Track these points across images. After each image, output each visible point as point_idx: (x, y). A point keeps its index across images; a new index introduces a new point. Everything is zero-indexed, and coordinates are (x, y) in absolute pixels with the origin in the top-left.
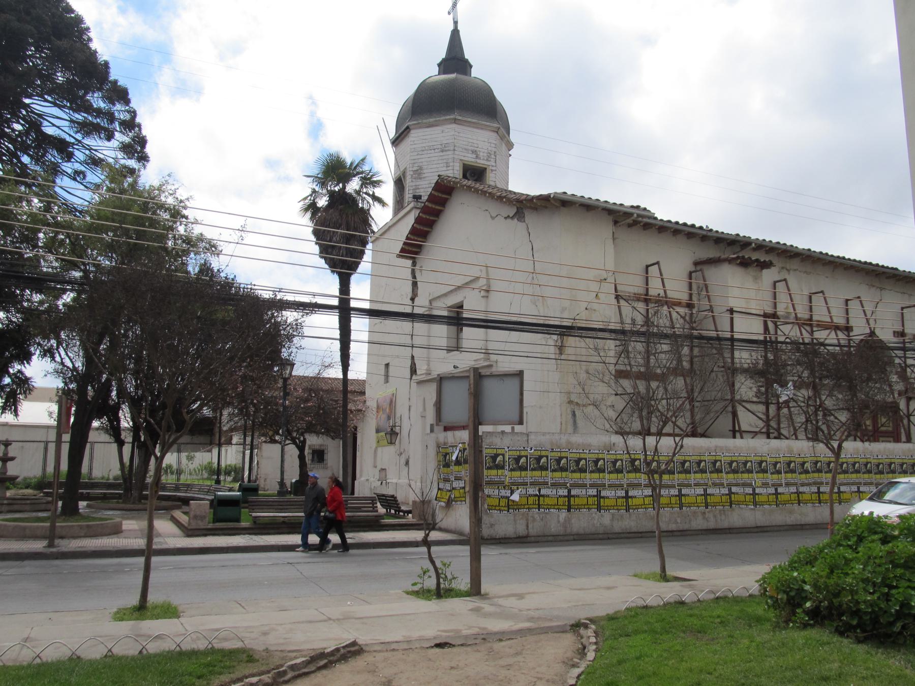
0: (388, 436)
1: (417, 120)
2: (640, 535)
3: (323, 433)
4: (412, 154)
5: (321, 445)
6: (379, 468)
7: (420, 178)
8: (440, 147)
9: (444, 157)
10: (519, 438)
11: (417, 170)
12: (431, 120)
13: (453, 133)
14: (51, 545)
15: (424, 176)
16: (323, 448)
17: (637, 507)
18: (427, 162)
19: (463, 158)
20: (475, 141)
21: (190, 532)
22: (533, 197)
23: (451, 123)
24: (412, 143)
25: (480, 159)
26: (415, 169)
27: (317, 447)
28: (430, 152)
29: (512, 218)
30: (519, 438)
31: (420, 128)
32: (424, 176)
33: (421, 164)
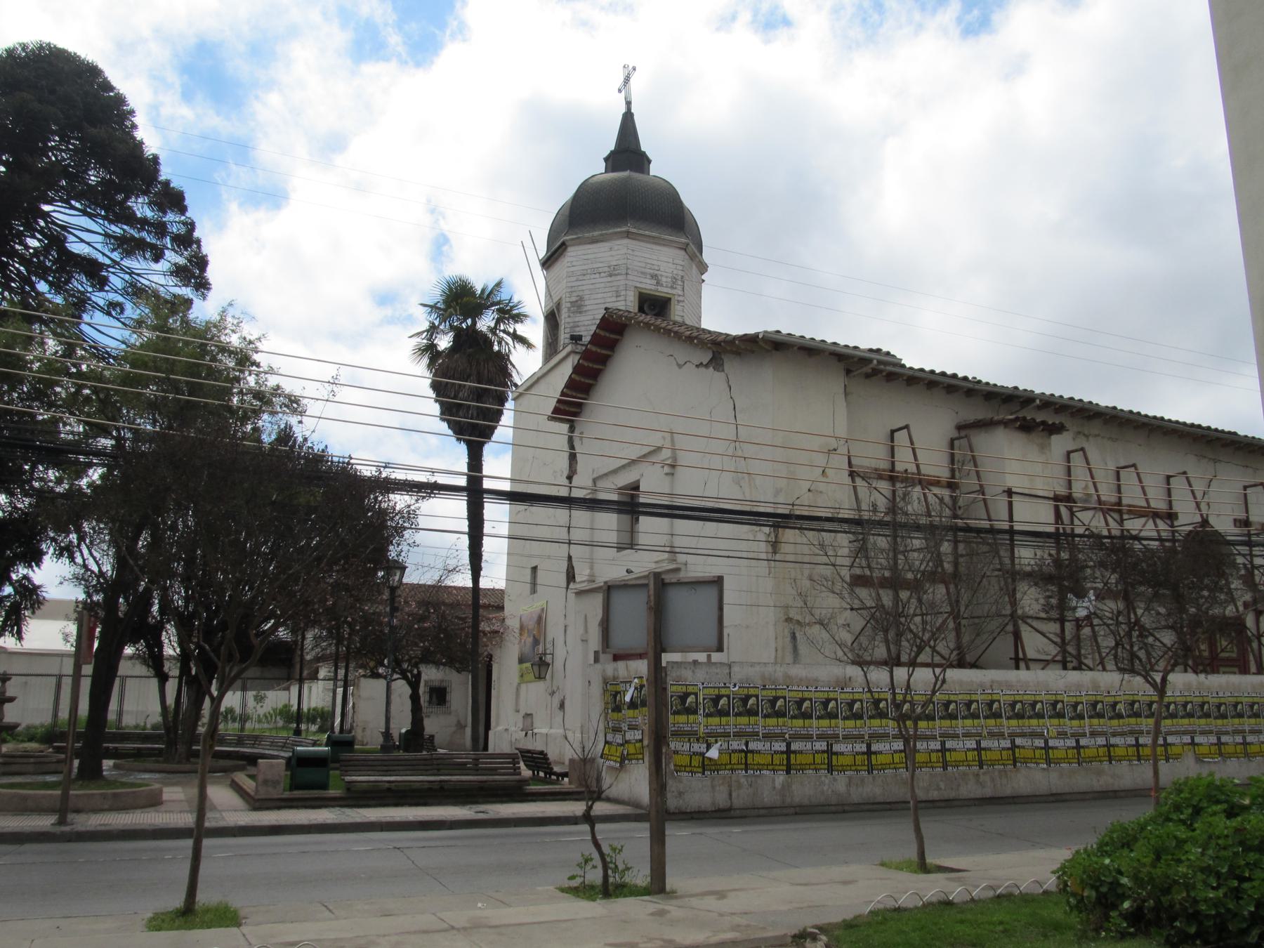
0: (536, 668)
1: (576, 234)
2: (888, 806)
3: (444, 664)
4: (569, 279)
5: (442, 681)
6: (522, 713)
7: (580, 312)
8: (606, 269)
9: (615, 284)
10: (718, 671)
11: (577, 301)
12: (596, 233)
13: (625, 251)
14: (62, 822)
15: (585, 309)
16: (444, 684)
17: (883, 767)
18: (590, 290)
19: (638, 285)
20: (655, 262)
21: (257, 804)
22: (736, 338)
23: (622, 238)
24: (569, 264)
25: (662, 285)
26: (574, 299)
27: (437, 684)
28: (593, 276)
29: (707, 366)
30: (718, 671)
31: (580, 244)
32: (585, 309)
33: (581, 293)
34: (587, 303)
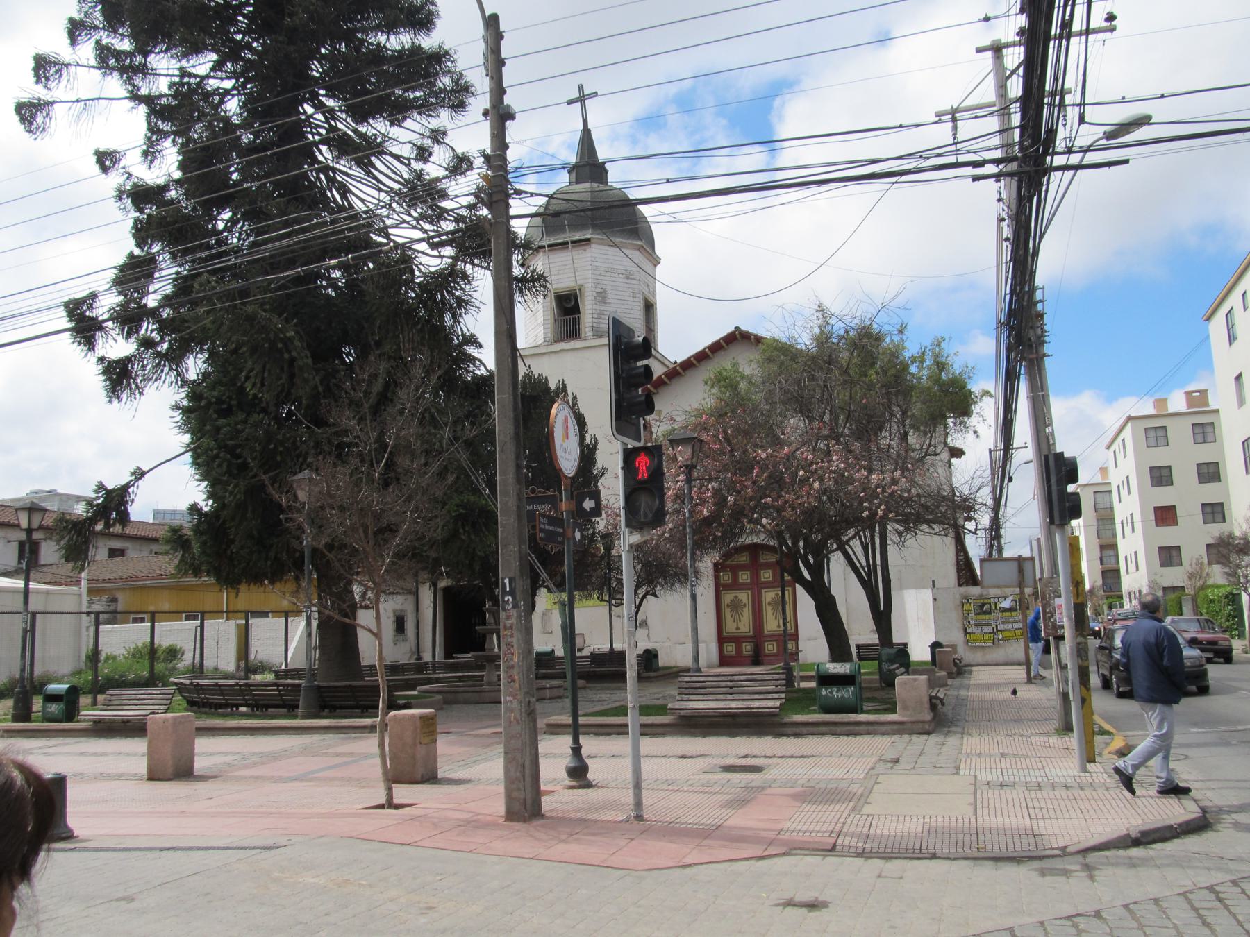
5: (401, 611)
15: (608, 301)
26: (599, 290)
31: (602, 244)
32: (608, 301)
34: (610, 296)
